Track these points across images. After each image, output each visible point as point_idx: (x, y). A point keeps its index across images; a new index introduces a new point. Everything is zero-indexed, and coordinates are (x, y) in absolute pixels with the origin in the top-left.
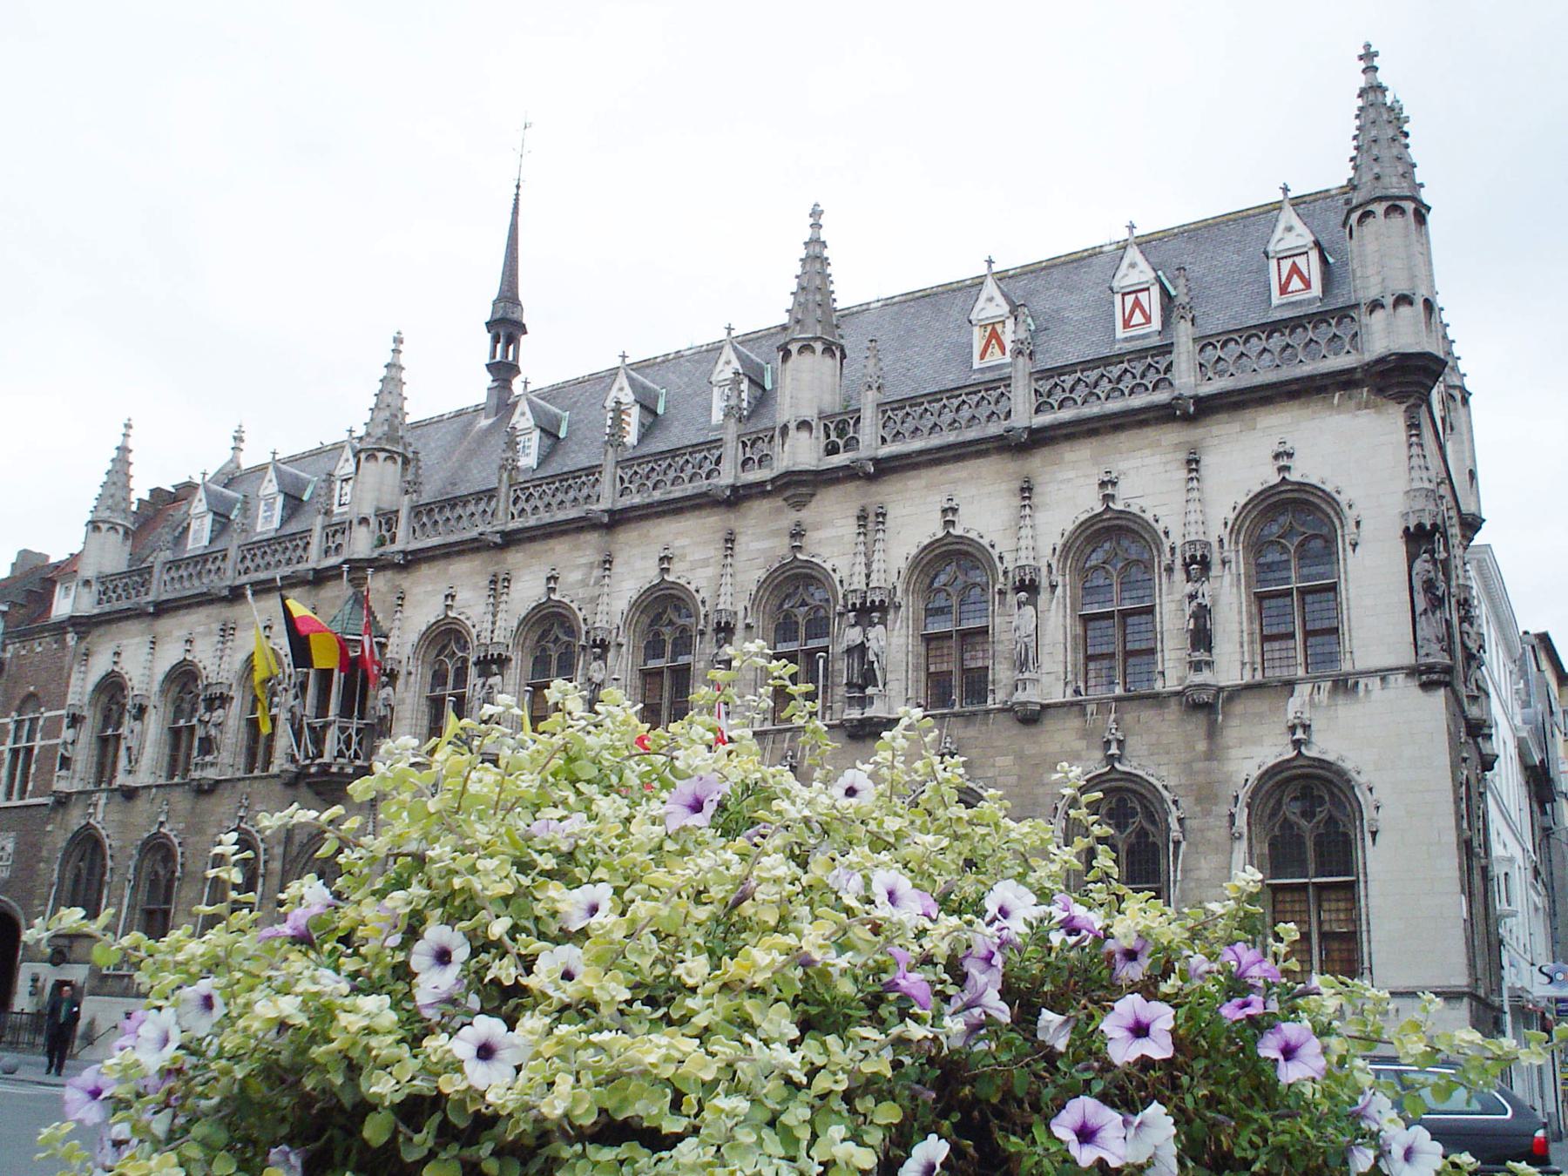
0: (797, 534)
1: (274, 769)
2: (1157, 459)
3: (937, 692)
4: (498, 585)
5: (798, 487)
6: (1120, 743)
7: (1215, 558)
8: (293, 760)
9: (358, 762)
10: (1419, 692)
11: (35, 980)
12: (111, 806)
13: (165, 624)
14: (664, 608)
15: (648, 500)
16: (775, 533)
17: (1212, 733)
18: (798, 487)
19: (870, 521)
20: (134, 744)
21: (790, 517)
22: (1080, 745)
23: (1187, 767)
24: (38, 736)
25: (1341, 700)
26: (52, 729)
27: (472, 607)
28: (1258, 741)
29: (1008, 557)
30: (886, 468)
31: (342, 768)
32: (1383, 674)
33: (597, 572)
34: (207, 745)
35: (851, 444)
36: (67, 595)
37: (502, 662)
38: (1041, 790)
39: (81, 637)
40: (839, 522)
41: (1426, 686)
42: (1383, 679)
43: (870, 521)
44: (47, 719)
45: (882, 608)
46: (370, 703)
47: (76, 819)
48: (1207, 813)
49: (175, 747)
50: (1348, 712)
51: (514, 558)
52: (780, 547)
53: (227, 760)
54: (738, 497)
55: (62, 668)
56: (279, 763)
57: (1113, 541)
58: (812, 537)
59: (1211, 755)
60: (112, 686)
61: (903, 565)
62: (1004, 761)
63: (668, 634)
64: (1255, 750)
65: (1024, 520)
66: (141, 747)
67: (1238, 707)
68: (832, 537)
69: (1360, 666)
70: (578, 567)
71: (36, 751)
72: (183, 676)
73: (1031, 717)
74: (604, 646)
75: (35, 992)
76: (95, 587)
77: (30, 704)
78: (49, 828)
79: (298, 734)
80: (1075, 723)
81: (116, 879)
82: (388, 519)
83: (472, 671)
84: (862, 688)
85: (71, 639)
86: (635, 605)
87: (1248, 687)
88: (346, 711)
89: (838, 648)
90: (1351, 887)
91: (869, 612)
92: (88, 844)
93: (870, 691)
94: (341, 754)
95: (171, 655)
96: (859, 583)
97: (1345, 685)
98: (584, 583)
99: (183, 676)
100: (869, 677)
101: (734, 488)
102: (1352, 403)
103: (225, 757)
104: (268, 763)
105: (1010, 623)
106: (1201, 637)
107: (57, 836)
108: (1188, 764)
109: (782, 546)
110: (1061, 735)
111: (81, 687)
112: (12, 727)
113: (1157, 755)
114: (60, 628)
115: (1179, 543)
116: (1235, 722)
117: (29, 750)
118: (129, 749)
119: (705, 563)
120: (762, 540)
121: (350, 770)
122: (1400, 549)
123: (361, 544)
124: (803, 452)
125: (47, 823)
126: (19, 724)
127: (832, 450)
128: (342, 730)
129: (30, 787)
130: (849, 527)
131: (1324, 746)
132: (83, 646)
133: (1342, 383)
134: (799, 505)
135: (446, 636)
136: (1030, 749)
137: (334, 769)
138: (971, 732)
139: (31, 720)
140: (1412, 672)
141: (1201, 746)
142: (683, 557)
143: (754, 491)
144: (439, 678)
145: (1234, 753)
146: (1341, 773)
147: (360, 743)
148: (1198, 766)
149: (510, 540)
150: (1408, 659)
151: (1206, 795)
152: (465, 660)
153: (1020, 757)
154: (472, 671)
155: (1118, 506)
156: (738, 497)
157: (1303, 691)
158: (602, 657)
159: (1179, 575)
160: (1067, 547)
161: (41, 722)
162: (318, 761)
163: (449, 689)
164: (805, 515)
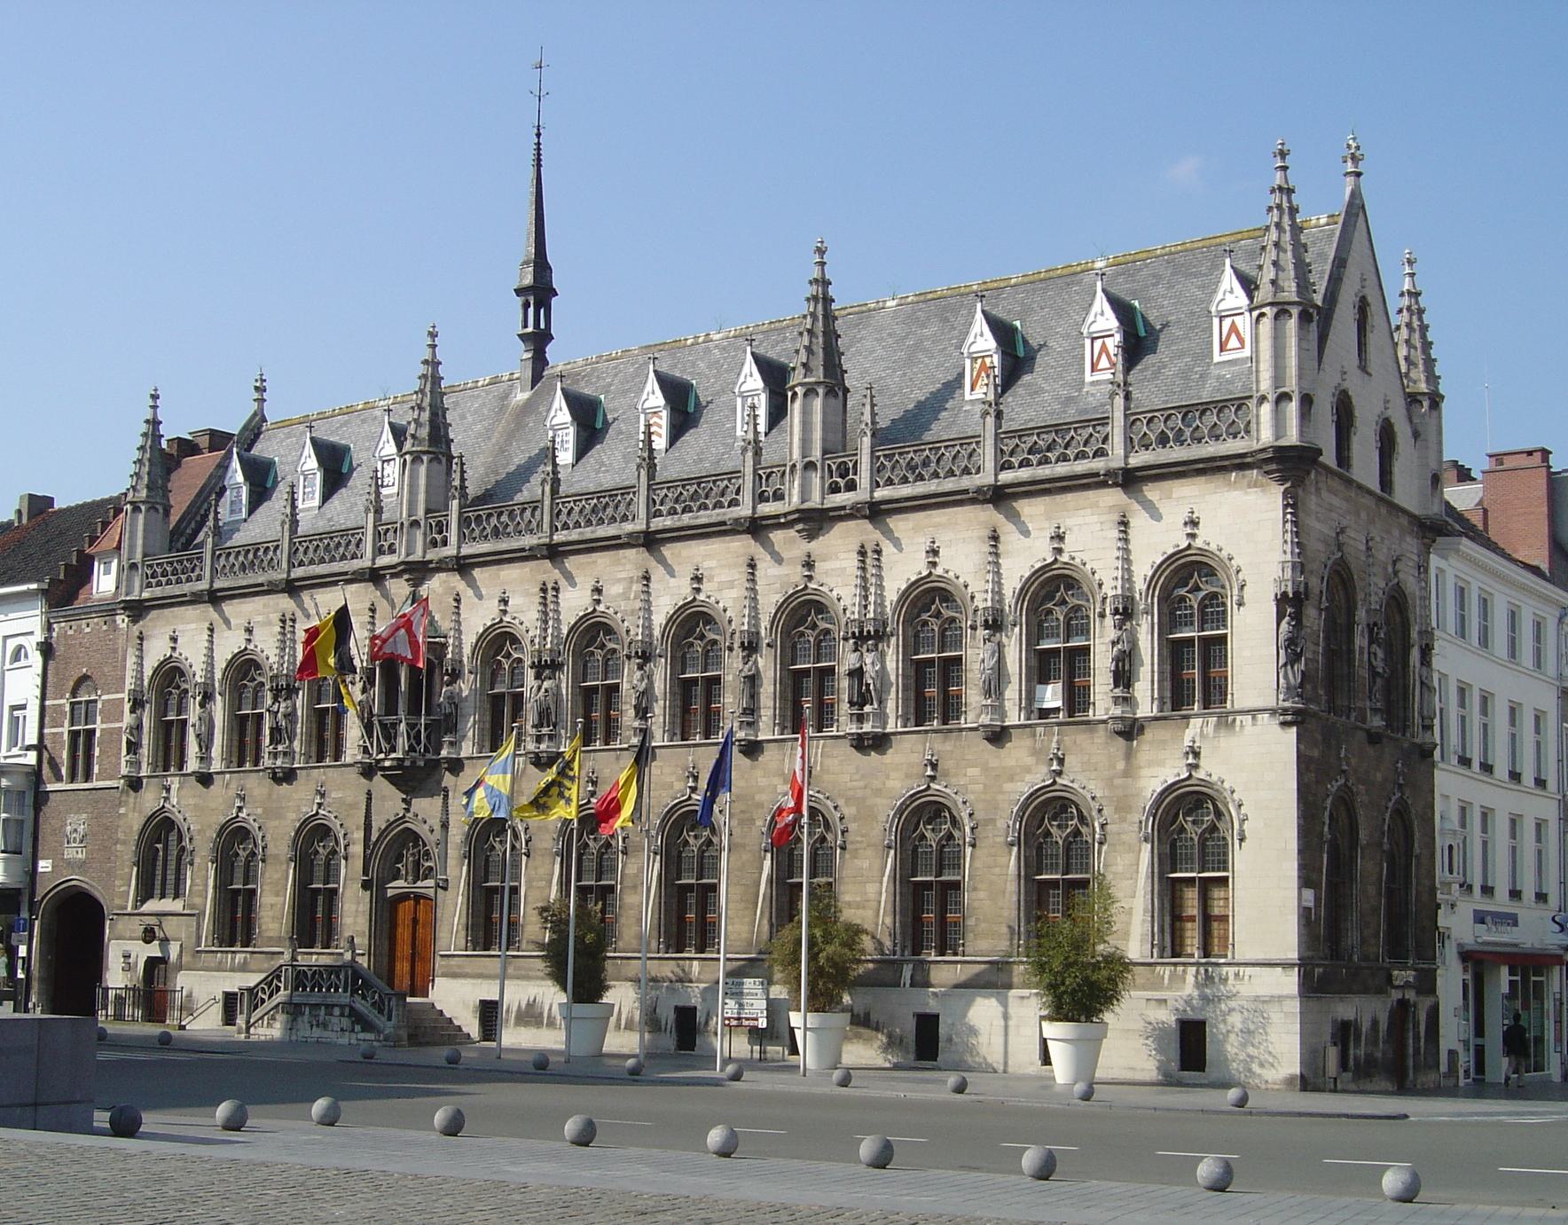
2: (1095, 518)
3: (918, 713)
6: (1061, 761)
8: (366, 751)
9: (429, 756)
10: (1278, 728)
11: (127, 956)
12: (184, 792)
15: (679, 524)
17: (1129, 755)
22: (1030, 761)
23: (1109, 783)
24: (99, 719)
25: (1223, 732)
28: (1161, 764)
29: (978, 597)
31: (413, 762)
32: (1254, 712)
36: (107, 572)
38: (1000, 797)
39: (135, 619)
40: (842, 556)
41: (1284, 724)
42: (1254, 718)
44: (104, 702)
47: (149, 800)
48: (1123, 820)
50: (1227, 742)
52: (795, 574)
55: (115, 651)
56: (352, 753)
59: (1129, 773)
60: (170, 674)
64: (1159, 770)
68: (836, 565)
69: (1237, 707)
70: (619, 580)
71: (98, 734)
75: (128, 968)
77: (82, 690)
78: (122, 811)
79: (368, 728)
80: (1028, 742)
81: (197, 860)
84: (861, 707)
85: (122, 620)
87: (1156, 719)
88: (414, 710)
89: (843, 669)
90: (1226, 879)
92: (161, 828)
93: (867, 708)
94: (412, 749)
97: (1226, 722)
98: (625, 596)
102: (1245, 482)
105: (976, 654)
107: (133, 815)
108: (1111, 779)
109: (795, 574)
110: (1017, 752)
112: (67, 708)
113: (1089, 769)
114: (108, 610)
115: (1111, 593)
116: (1145, 747)
121: (422, 764)
122: (1273, 608)
125: (120, 805)
127: (835, 489)
128: (411, 726)
129: (96, 769)
131: (1211, 768)
132: (136, 629)
133: (1238, 463)
134: (811, 536)
135: (499, 640)
136: (994, 763)
137: (407, 763)
138: (948, 746)
139: (88, 702)
140: (1273, 712)
141: (1121, 765)
142: (711, 579)
145: (1145, 772)
147: (428, 737)
148: (1118, 781)
150: (1272, 703)
152: (520, 660)
153: (986, 769)
154: (530, 674)
157: (1196, 723)
159: (1109, 621)
161: (99, 705)
162: (393, 755)
164: (815, 546)
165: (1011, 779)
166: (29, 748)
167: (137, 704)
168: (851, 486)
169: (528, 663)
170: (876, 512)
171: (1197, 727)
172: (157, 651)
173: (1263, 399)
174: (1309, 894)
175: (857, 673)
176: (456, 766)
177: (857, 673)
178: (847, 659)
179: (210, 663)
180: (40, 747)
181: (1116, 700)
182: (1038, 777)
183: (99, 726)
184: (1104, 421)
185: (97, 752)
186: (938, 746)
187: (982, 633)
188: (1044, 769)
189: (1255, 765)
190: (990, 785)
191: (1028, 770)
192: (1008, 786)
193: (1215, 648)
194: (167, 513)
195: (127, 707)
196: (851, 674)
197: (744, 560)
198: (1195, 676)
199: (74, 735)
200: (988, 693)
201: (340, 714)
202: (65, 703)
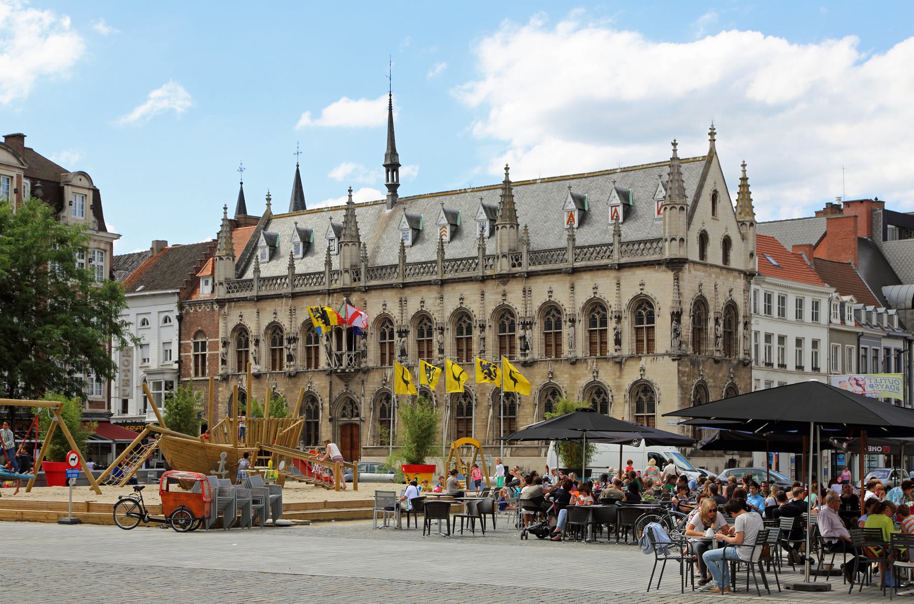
1: (320, 368)
4: (403, 302)
5: (504, 278)
6: (597, 372)
7: (624, 315)
14: (462, 318)
16: (497, 293)
17: (621, 369)
18: (504, 278)
19: (526, 292)
20: (257, 356)
21: (502, 288)
22: (586, 372)
27: (394, 311)
30: (530, 275)
33: (438, 301)
34: (290, 358)
35: (520, 265)
37: (407, 332)
45: (531, 324)
46: (357, 345)
49: (274, 357)
51: (408, 292)
54: (484, 279)
57: (596, 310)
58: (509, 296)
59: (620, 377)
61: (537, 309)
62: (567, 376)
63: (464, 326)
64: (631, 375)
65: (571, 297)
66: (260, 357)
67: (628, 363)
68: (515, 297)
72: (275, 329)
73: (574, 362)
74: (442, 329)
76: (225, 285)
83: (396, 335)
86: (452, 315)
89: (517, 336)
91: (527, 325)
96: (522, 314)
99: (275, 329)
101: (483, 277)
103: (299, 362)
104: (317, 366)
106: (618, 342)
109: (499, 298)
113: (607, 376)
117: (204, 356)
118: (255, 358)
119: (475, 301)
126: (196, 344)
130: (520, 294)
131: (648, 376)
134: (505, 284)
141: (618, 374)
143: (490, 278)
144: (383, 336)
146: (652, 384)
151: (619, 388)
152: (392, 329)
153: (570, 374)
155: (598, 296)
156: (484, 279)
158: (442, 333)
160: (584, 308)
163: (387, 340)
164: (506, 287)
165: (580, 379)
166: (176, 362)
167: (225, 344)
168: (520, 265)
169: (395, 330)
170: (530, 275)
171: (645, 362)
172: (233, 321)
173: (666, 240)
175: (523, 338)
176: (367, 371)
177: (523, 338)
178: (519, 332)
179: (259, 327)
180: (179, 362)
181: (616, 351)
182: (590, 378)
183: (207, 352)
184: (611, 245)
185: (207, 364)
186: (553, 366)
187: (569, 324)
188: (591, 375)
191: (585, 375)
192: (578, 382)
194: (234, 257)
195: (221, 345)
196: (520, 338)
197: (479, 292)
198: (645, 342)
199: (196, 356)
200: (571, 347)
201: (317, 348)
202: (190, 342)
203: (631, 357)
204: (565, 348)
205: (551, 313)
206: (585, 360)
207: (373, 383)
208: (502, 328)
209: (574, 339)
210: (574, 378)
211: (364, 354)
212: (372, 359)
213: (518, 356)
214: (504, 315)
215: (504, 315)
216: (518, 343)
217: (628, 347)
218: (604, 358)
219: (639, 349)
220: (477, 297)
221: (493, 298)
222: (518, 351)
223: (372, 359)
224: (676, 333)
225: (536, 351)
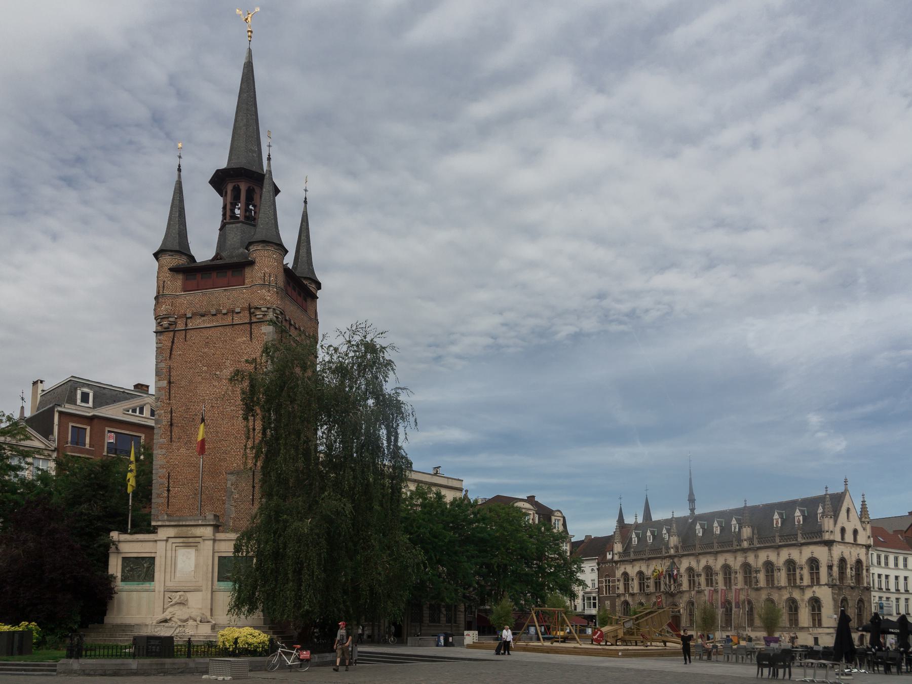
0: (746, 558)
4: (698, 562)
5: (745, 551)
13: (635, 563)
14: (726, 568)
26: (614, 581)
43: (756, 557)
51: (700, 557)
53: (652, 589)
54: (736, 551)
56: (662, 589)
60: (625, 574)
64: (809, 594)
65: (779, 558)
68: (751, 559)
82: (676, 548)
91: (757, 571)
95: (637, 569)
100: (757, 581)
106: (802, 579)
111: (619, 573)
113: (796, 595)
120: (740, 559)
123: (672, 552)
124: (745, 544)
131: (817, 595)
135: (690, 570)
143: (739, 550)
144: (690, 576)
149: (700, 554)
151: (803, 600)
171: (815, 588)
174: (835, 616)
175: (756, 577)
180: (599, 588)
189: (825, 594)
190: (781, 598)
193: (818, 573)
203: (808, 586)
204: (776, 582)
205: (769, 566)
206: (785, 587)
207: (686, 598)
208: (745, 573)
209: (782, 578)
210: (781, 596)
211: (681, 585)
212: (685, 586)
213: (753, 586)
214: (746, 567)
215: (746, 567)
216: (754, 580)
217: (807, 581)
218: (795, 586)
219: (812, 582)
220: (733, 559)
221: (740, 559)
222: (753, 583)
223: (685, 586)
224: (830, 575)
225: (762, 583)
